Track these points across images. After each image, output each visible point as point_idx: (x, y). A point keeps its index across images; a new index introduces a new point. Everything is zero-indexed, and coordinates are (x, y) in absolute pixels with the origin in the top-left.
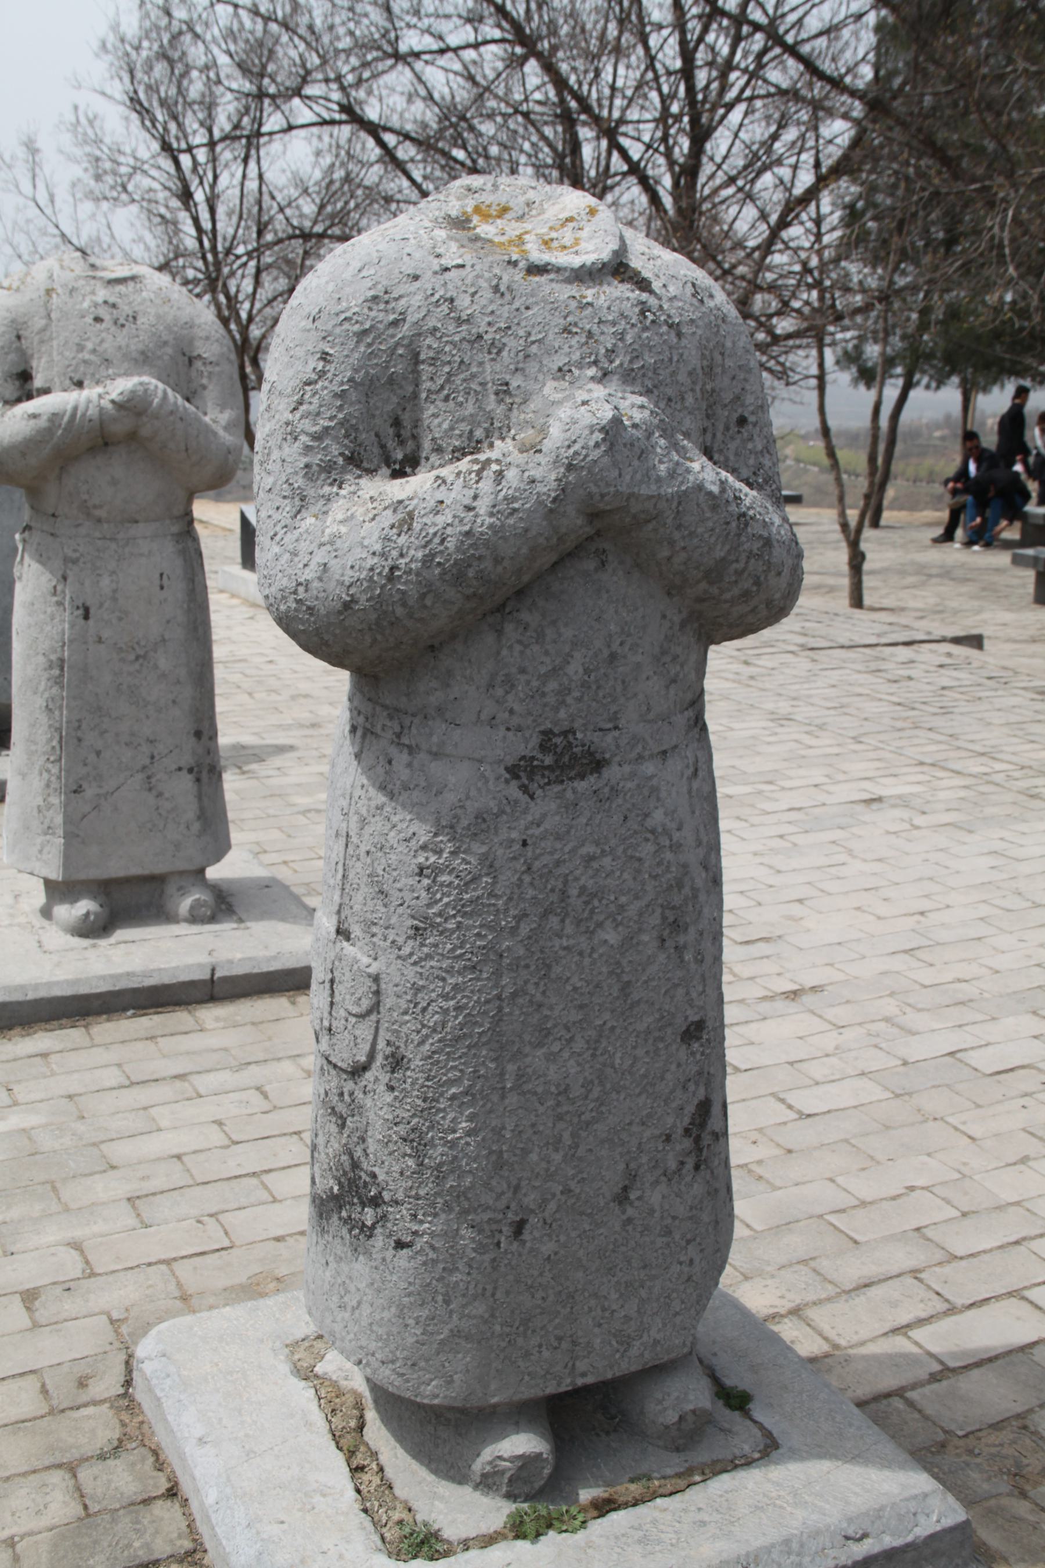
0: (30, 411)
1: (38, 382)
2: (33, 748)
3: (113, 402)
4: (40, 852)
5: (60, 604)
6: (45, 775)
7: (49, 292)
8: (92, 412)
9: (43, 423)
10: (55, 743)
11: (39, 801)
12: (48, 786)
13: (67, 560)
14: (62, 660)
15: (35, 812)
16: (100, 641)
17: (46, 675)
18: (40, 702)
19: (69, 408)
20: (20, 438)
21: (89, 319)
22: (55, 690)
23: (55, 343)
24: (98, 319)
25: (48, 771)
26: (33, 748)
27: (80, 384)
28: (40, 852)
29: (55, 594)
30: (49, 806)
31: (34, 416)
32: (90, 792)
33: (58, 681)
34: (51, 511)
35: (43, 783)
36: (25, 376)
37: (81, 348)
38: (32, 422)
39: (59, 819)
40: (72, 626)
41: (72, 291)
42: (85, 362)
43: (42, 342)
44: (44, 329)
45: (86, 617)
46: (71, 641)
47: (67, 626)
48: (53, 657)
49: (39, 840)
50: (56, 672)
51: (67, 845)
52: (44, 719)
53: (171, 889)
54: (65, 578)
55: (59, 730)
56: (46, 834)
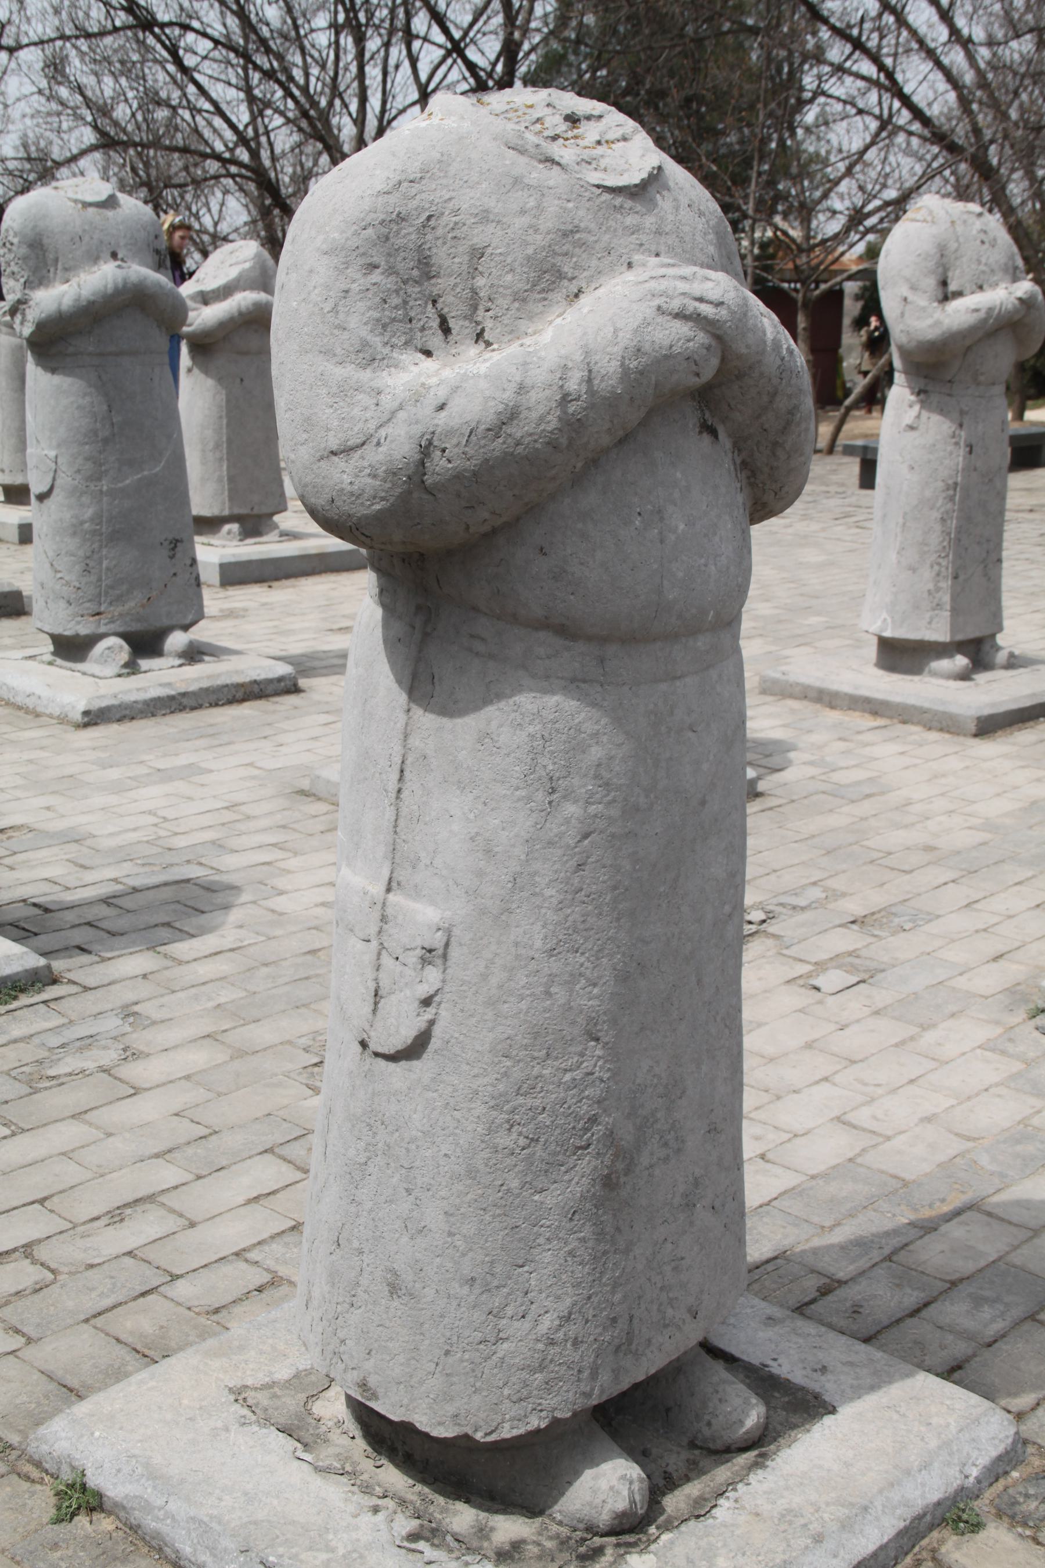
0: (973, 307)
1: (953, 287)
2: (926, 549)
3: (1020, 299)
4: (930, 623)
5: (957, 444)
6: (936, 568)
7: (953, 222)
8: (1010, 306)
9: (982, 315)
10: (945, 544)
11: (931, 586)
12: (938, 575)
13: (962, 413)
14: (956, 484)
15: (926, 595)
16: (975, 469)
17: (944, 495)
18: (936, 515)
19: (998, 303)
20: (966, 326)
21: (978, 242)
22: (949, 506)
23: (964, 259)
24: (983, 242)
25: (939, 564)
26: (926, 549)
27: (981, 288)
28: (930, 623)
29: (953, 437)
30: (938, 589)
31: (977, 310)
32: (962, 578)
33: (952, 499)
34: (949, 378)
35: (934, 574)
36: (944, 283)
37: (979, 262)
38: (975, 315)
39: (947, 598)
40: (964, 458)
41: (965, 222)
42: (983, 272)
43: (956, 258)
44: (956, 250)
45: (970, 452)
46: (963, 470)
47: (961, 459)
48: (950, 482)
49: (928, 615)
50: (951, 492)
51: (952, 616)
52: (938, 527)
53: (986, 647)
54: (961, 426)
55: (949, 534)
56: (933, 609)
